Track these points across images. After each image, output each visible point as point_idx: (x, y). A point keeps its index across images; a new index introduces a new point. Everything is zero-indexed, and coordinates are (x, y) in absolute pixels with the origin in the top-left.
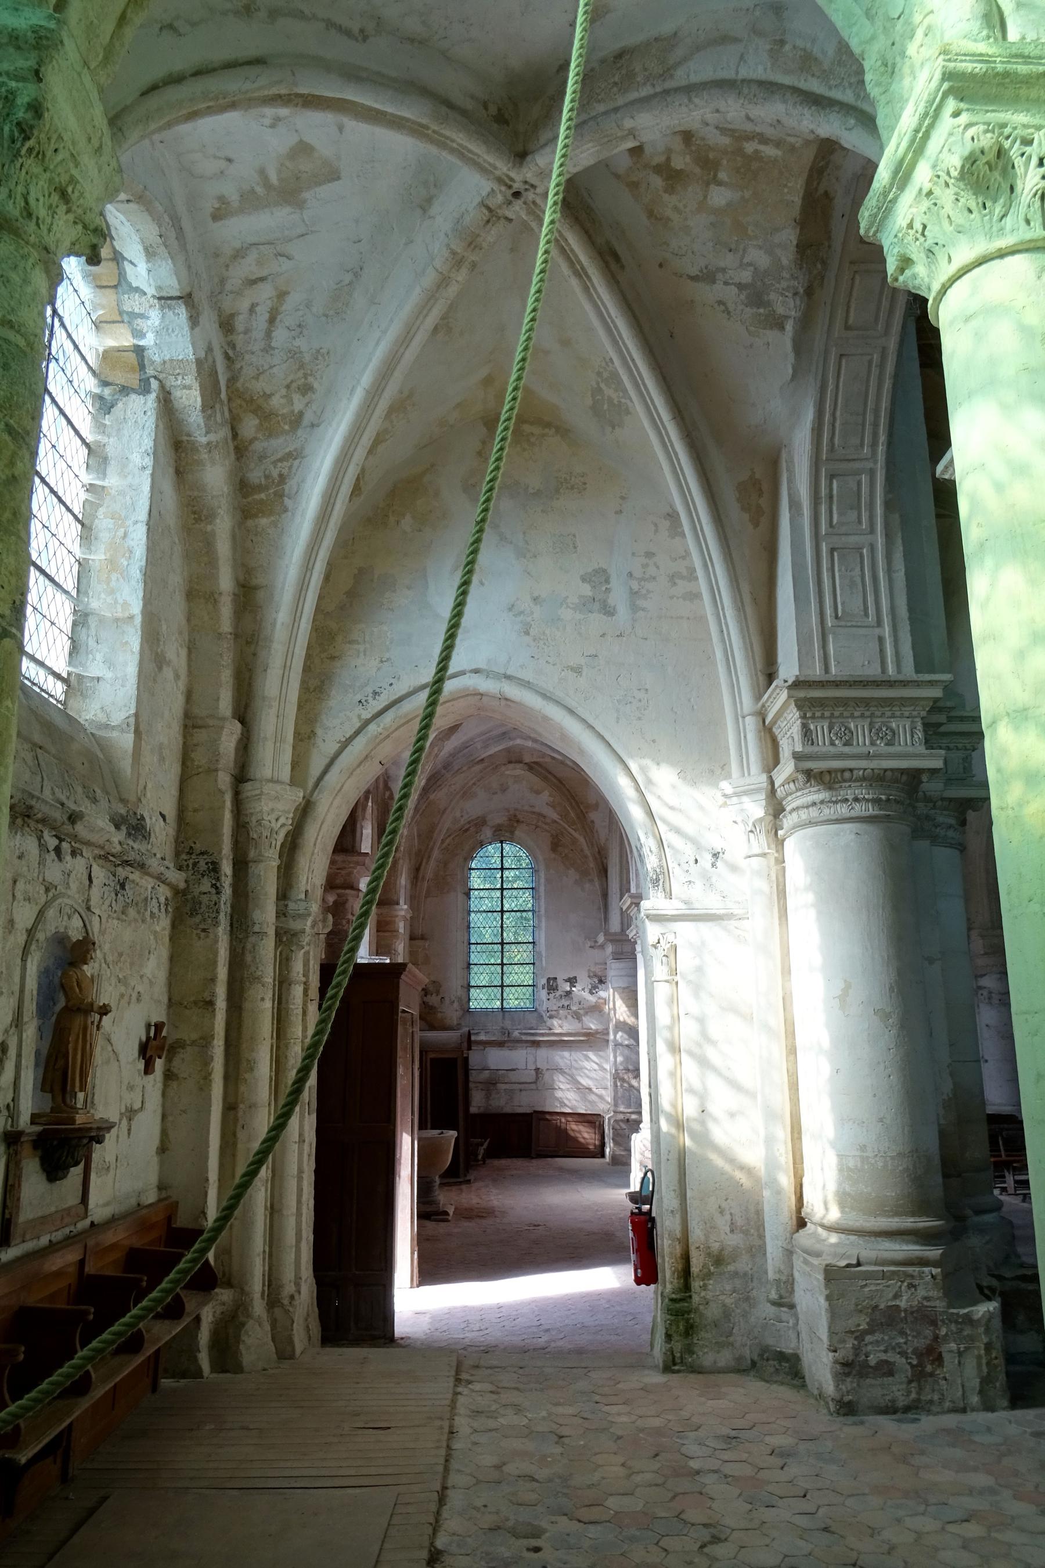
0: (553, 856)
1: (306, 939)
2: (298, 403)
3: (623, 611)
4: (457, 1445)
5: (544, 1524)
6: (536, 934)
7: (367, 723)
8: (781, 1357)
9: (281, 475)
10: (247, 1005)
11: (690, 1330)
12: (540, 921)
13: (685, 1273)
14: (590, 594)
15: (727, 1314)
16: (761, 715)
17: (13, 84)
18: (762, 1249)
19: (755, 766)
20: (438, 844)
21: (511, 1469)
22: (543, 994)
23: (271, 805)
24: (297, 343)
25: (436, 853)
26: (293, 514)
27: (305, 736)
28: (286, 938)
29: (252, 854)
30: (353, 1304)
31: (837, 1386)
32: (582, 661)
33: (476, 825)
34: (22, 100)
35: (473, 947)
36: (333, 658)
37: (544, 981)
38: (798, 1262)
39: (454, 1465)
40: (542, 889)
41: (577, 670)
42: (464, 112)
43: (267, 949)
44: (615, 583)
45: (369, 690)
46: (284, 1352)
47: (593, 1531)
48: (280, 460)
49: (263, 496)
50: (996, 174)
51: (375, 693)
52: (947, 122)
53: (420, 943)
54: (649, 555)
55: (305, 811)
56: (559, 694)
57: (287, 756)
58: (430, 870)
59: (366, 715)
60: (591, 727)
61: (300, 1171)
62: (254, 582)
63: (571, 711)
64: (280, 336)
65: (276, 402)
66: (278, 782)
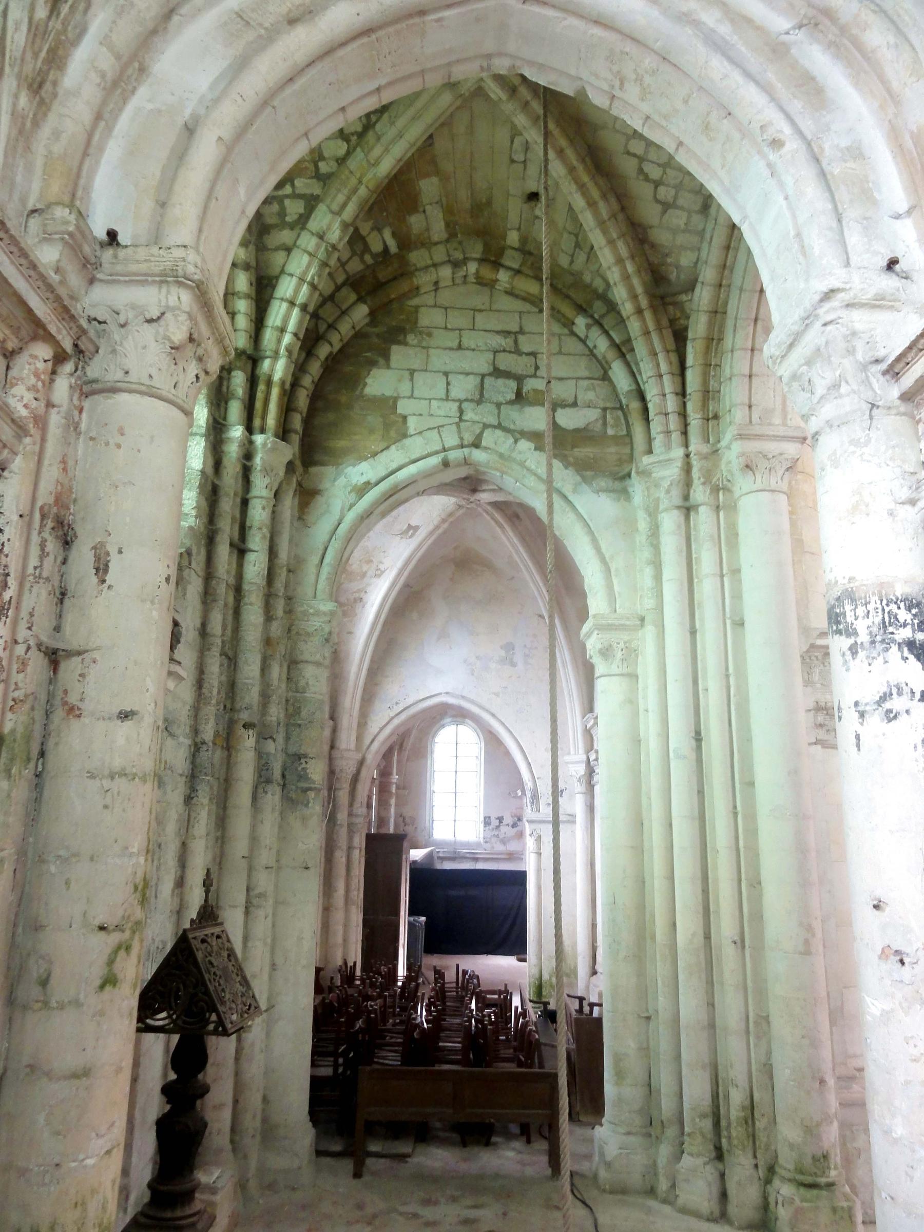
1: (360, 826)
2: (365, 568)
3: (520, 666)
7: (392, 718)
19: (581, 750)
27: (362, 724)
28: (351, 826)
41: (497, 694)
43: (343, 833)
45: (394, 701)
51: (397, 703)
55: (361, 763)
56: (487, 706)
59: (392, 714)
61: (357, 941)
63: (493, 715)
66: (349, 750)
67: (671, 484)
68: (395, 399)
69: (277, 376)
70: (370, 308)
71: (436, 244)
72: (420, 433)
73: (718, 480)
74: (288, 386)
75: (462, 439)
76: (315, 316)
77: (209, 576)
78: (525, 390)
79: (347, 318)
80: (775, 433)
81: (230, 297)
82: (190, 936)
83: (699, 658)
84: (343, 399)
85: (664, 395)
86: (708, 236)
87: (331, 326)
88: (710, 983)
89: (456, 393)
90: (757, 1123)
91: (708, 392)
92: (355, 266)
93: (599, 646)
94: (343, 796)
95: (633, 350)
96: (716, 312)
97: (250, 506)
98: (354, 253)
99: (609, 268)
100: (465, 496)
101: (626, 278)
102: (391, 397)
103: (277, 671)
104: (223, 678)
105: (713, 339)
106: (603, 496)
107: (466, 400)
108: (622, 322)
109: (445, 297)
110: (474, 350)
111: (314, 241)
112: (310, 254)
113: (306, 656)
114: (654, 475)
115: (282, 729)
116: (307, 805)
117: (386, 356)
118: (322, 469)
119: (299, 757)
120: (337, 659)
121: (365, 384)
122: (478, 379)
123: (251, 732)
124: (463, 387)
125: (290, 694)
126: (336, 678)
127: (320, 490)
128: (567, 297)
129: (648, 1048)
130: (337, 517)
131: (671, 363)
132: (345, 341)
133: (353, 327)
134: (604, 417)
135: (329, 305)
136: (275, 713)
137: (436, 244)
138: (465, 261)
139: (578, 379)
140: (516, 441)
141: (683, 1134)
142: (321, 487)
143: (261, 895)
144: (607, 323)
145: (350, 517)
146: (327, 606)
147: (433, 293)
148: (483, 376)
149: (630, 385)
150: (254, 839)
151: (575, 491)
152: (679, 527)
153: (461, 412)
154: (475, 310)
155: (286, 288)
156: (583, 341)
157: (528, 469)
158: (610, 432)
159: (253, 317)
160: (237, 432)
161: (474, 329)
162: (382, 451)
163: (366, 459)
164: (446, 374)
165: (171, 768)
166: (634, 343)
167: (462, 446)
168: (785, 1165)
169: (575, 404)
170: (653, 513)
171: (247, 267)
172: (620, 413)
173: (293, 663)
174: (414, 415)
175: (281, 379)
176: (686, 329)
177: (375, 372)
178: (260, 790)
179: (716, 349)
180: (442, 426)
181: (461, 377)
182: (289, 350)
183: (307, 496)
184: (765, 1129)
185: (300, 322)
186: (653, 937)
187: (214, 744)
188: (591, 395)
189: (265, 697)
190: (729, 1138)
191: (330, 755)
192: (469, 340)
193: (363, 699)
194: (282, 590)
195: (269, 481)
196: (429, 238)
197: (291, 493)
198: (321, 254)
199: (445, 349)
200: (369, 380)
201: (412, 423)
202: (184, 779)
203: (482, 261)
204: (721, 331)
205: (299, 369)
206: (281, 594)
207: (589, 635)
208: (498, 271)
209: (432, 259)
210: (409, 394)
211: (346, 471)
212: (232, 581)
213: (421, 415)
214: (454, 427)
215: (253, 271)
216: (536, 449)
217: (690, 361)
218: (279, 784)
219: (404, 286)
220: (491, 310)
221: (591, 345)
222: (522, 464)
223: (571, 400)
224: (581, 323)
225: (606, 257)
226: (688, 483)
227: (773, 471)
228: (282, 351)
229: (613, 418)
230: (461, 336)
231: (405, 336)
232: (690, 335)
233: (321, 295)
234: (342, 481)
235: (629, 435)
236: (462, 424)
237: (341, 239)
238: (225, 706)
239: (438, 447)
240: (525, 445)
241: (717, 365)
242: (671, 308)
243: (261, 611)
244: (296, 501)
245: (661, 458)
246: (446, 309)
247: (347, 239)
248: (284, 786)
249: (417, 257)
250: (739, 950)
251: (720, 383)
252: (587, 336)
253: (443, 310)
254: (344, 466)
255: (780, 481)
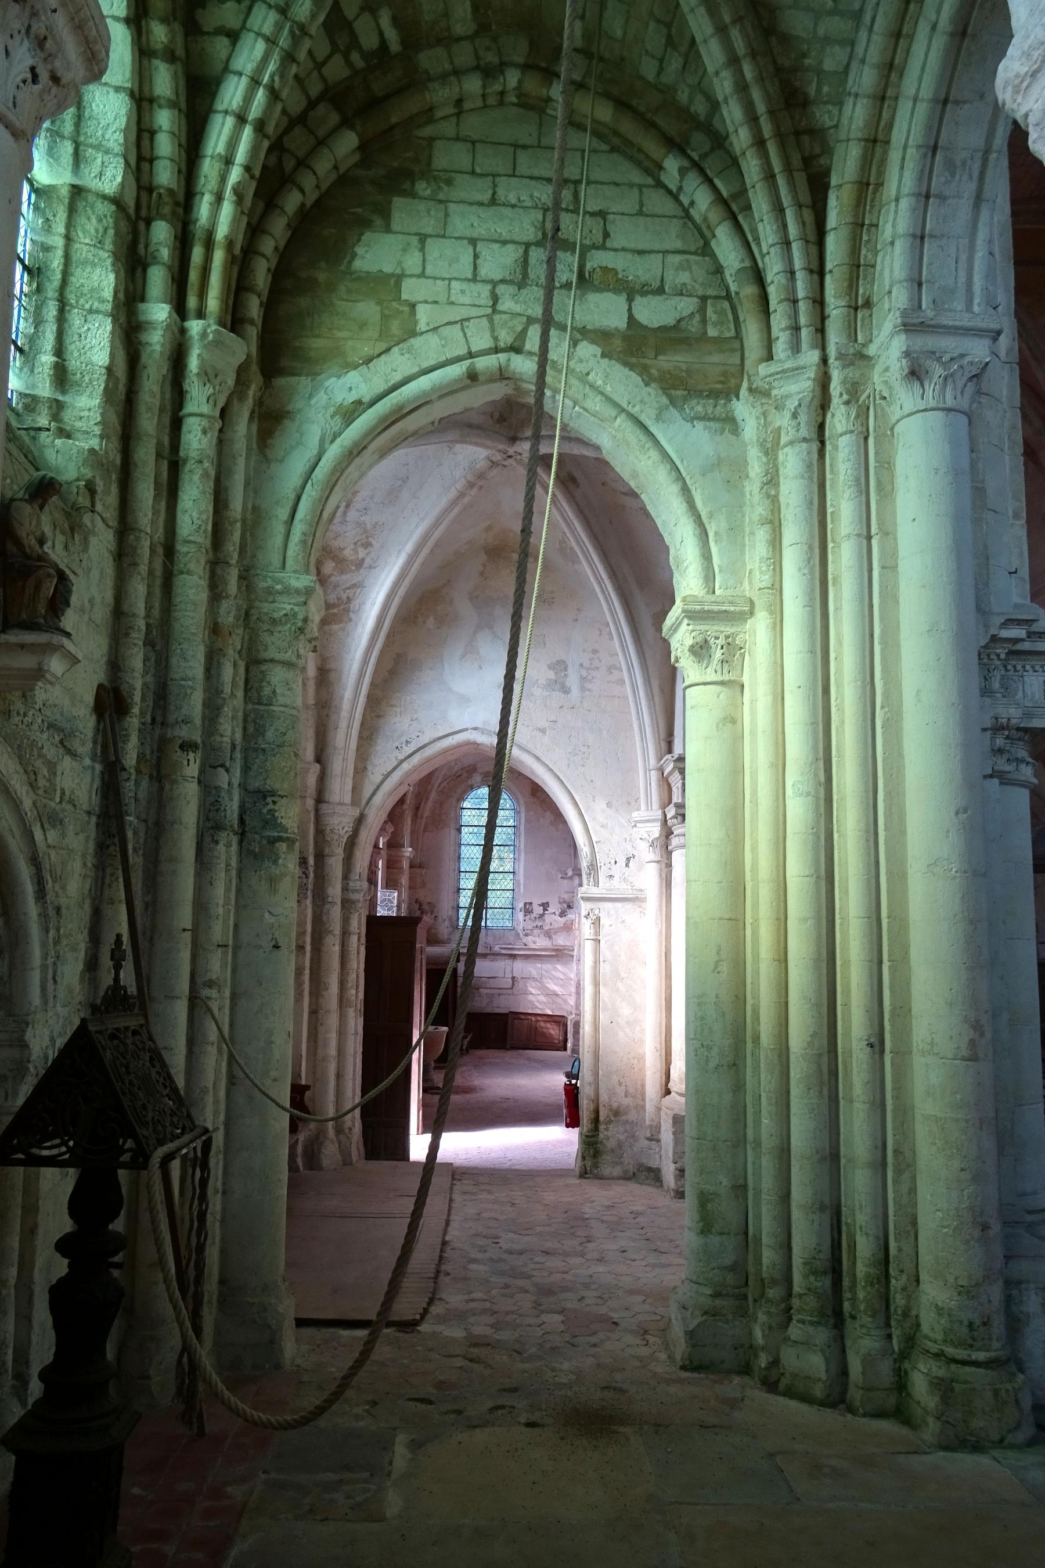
0: (532, 800)
4: (454, 1205)
5: (501, 1234)
6: (517, 865)
7: (402, 761)
8: (650, 1170)
9: (348, 598)
10: (324, 949)
11: (597, 1154)
12: (519, 855)
13: (596, 1121)
14: (554, 677)
15: (620, 1145)
16: (661, 770)
17: (296, 609)
18: (643, 1107)
19: (656, 805)
20: (435, 788)
21: (485, 1215)
22: (520, 916)
23: (339, 819)
24: (363, 518)
25: (433, 795)
26: (356, 625)
27: (361, 770)
28: (347, 904)
29: (327, 851)
30: (384, 1134)
31: (676, 1183)
32: (547, 725)
33: (467, 771)
34: (301, 616)
35: (462, 874)
36: (379, 717)
37: (521, 905)
38: (663, 1114)
39: (453, 1212)
40: (522, 828)
41: (543, 731)
42: (478, 427)
43: (335, 913)
44: (570, 671)
45: (404, 739)
46: (347, 1162)
47: (526, 1238)
48: (348, 588)
49: (335, 611)
50: (704, 651)
52: (684, 627)
53: (417, 870)
54: (595, 651)
55: (360, 820)
57: (349, 787)
58: (427, 811)
59: (401, 757)
60: (551, 770)
61: (355, 1053)
62: (327, 667)
63: (538, 759)
64: (352, 515)
65: (347, 553)
67: (800, 405)
68: (399, 278)
69: (222, 231)
70: (360, 135)
71: (459, 39)
72: (435, 329)
73: (869, 397)
74: (237, 251)
75: (496, 339)
76: (277, 147)
77: (125, 527)
78: (589, 266)
79: (326, 151)
80: (957, 323)
81: (145, 105)
82: (92, 1028)
83: (832, 656)
84: (322, 277)
85: (792, 273)
86: (867, 18)
87: (303, 163)
88: (834, 1100)
89: (487, 270)
90: (893, 1281)
91: (859, 266)
92: (336, 70)
93: (689, 642)
94: (335, 864)
95: (748, 207)
96: (875, 141)
97: (185, 428)
98: (335, 49)
99: (717, 73)
100: (501, 447)
101: (742, 88)
102: (393, 275)
103: (229, 673)
104: (149, 678)
105: (868, 184)
106: (699, 425)
107: (503, 281)
108: (734, 164)
109: (472, 124)
110: (513, 206)
111: (273, 16)
112: (267, 40)
113: (272, 653)
114: (774, 392)
115: (238, 755)
116: (275, 862)
117: (385, 214)
118: (293, 380)
119: (264, 795)
120: (325, 677)
121: (354, 255)
122: (521, 250)
123: (191, 756)
124: (497, 262)
125: (250, 706)
126: (324, 709)
127: (288, 412)
128: (653, 125)
129: (744, 1187)
130: (315, 452)
131: (804, 224)
132: (325, 186)
133: (336, 167)
134: (702, 310)
135: (298, 130)
136: (229, 730)
137: (459, 39)
138: (502, 66)
139: (666, 252)
140: (574, 343)
141: (790, 1295)
142: (290, 407)
143: (210, 984)
144: (711, 166)
145: (333, 451)
146: (303, 581)
147: (454, 120)
148: (527, 245)
149: (743, 261)
150: (201, 906)
151: (658, 418)
152: (809, 466)
153: (495, 298)
154: (516, 146)
155: (232, 93)
156: (676, 197)
157: (591, 386)
158: (712, 332)
159: (184, 142)
160: (158, 312)
161: (514, 176)
162: (379, 355)
163: (356, 367)
164: (473, 242)
165: (71, 802)
166: (751, 193)
167: (496, 350)
168: (931, 1334)
169: (660, 291)
170: (770, 450)
171: (170, 57)
172: (726, 305)
173: (254, 662)
174: (426, 302)
175: (226, 237)
176: (827, 173)
177: (367, 236)
178: (207, 839)
179: (873, 200)
180: (468, 319)
181: (496, 246)
182: (238, 192)
183: (272, 420)
184: (904, 1289)
185: (254, 150)
186: (757, 1039)
187: (139, 772)
188: (684, 277)
189: (213, 707)
190: (853, 1299)
191: (317, 810)
192: (510, 191)
193: (361, 737)
194: (236, 556)
195: (211, 390)
196: (448, 29)
197: (246, 414)
198: (284, 41)
199: (471, 204)
200: (360, 250)
201: (424, 316)
202: (94, 819)
203: (526, 67)
204: (881, 173)
205: (254, 228)
206: (233, 562)
207: (675, 628)
208: (551, 84)
209: (452, 63)
210: (418, 271)
211: (327, 384)
212: (160, 535)
213: (436, 302)
214: (484, 322)
215: (179, 67)
216: (603, 356)
217: (832, 219)
218: (236, 833)
219: (412, 105)
220: (539, 147)
221: (686, 201)
222: (584, 377)
223: (656, 284)
224: (672, 165)
225: (712, 54)
226: (824, 404)
227: (950, 380)
228: (228, 193)
229: (715, 312)
230: (495, 186)
231: (413, 184)
232: (834, 181)
233: (284, 112)
234: (321, 398)
235: (738, 336)
236: (497, 317)
237: (313, 16)
238: (153, 719)
239: (462, 351)
240: (587, 350)
241: (872, 225)
242: (806, 139)
243: (204, 583)
244: (254, 428)
245: (788, 365)
246: (473, 143)
247: (322, 18)
248: (242, 835)
249: (429, 60)
250: (877, 1057)
251: (876, 254)
252: (680, 188)
253: (469, 145)
254: (322, 376)
255: (959, 397)
